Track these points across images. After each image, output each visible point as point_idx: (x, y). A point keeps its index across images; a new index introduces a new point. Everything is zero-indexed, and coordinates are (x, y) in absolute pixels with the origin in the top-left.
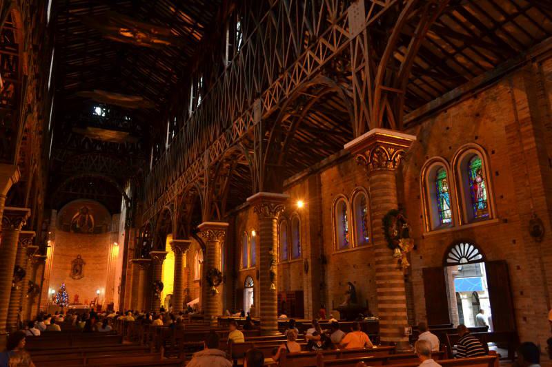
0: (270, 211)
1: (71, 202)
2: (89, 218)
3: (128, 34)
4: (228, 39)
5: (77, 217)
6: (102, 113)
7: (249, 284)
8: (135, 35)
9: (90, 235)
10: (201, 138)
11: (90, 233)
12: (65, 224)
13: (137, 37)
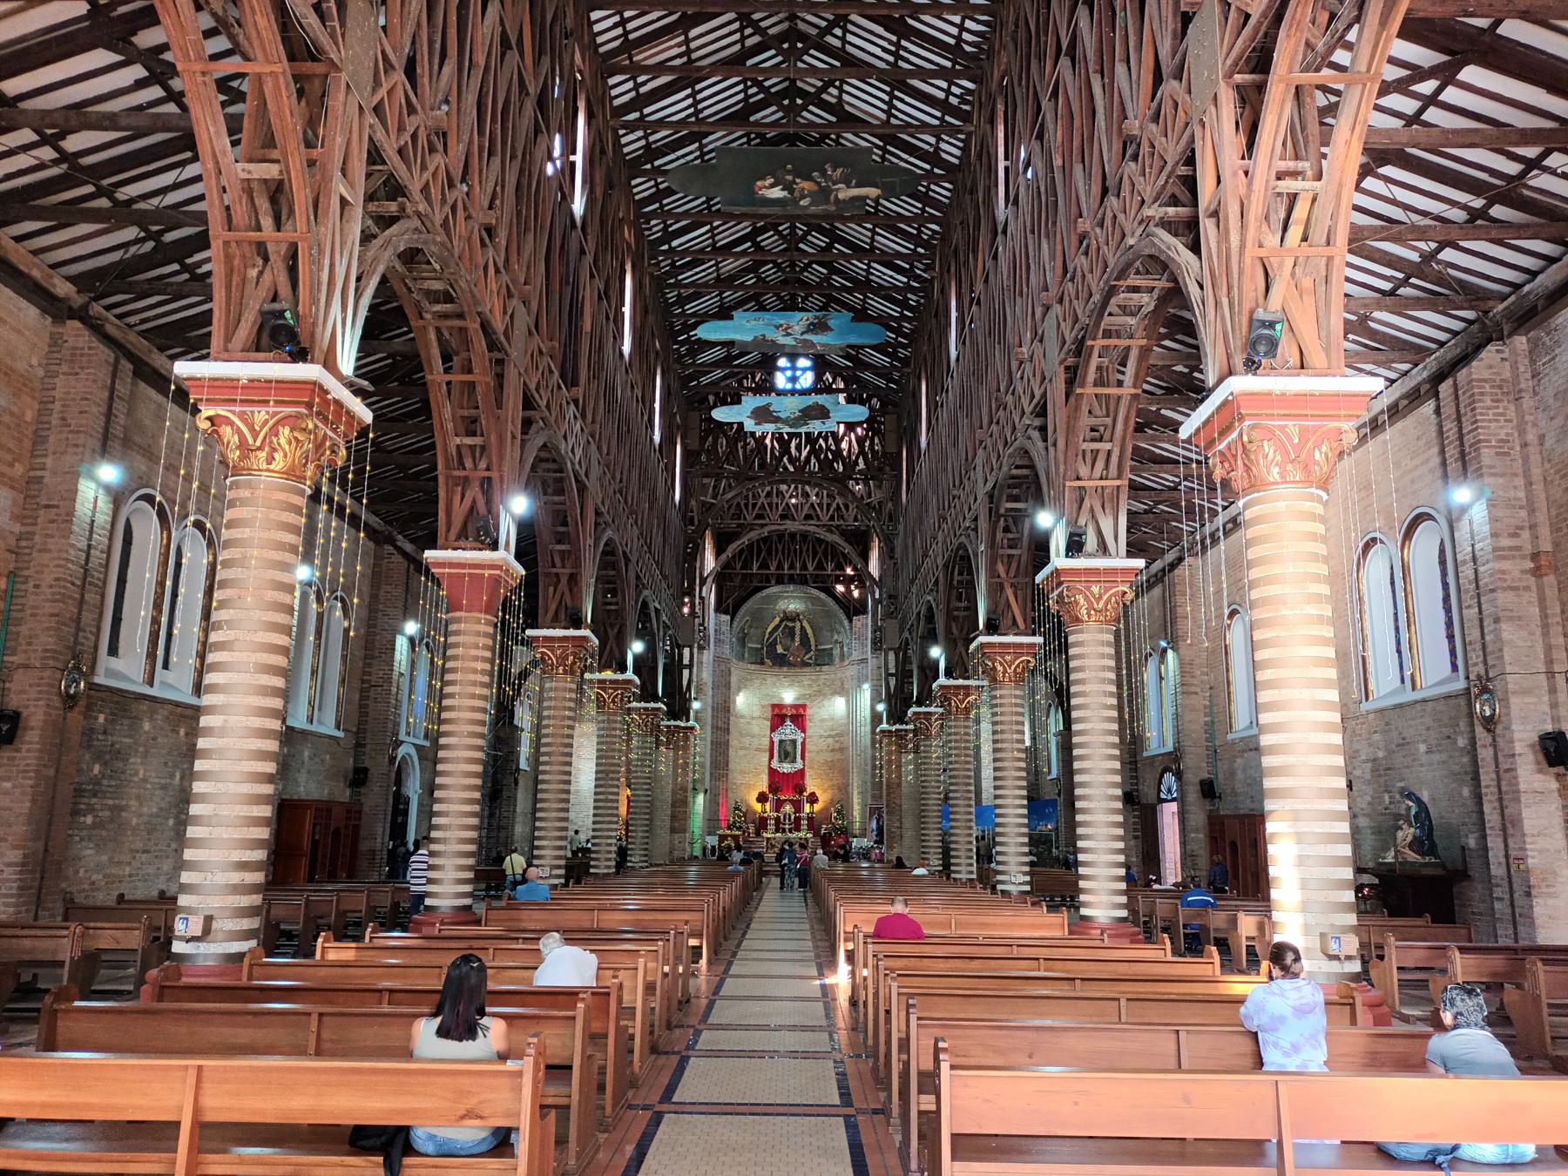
1: (759, 595)
2: (802, 626)
3: (777, 193)
4: (1001, 150)
5: (776, 628)
6: (804, 370)
7: (1169, 791)
8: (791, 191)
9: (807, 669)
10: (969, 415)
11: (808, 665)
13: (797, 194)
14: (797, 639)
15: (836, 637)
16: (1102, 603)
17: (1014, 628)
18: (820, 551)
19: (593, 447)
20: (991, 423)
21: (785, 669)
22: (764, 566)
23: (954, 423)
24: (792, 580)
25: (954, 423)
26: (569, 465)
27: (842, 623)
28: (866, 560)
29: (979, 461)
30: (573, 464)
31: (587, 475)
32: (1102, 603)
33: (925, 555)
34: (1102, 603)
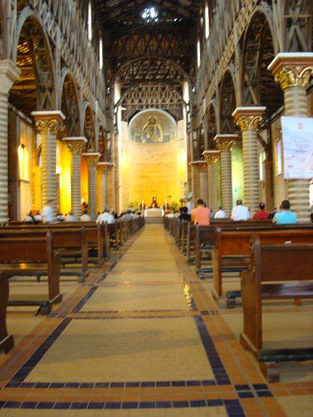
0: (295, 77)
5: (146, 127)
12: (136, 135)
14: (155, 131)
15: (171, 130)
16: (301, 74)
17: (252, 104)
18: (164, 94)
19: (58, 28)
20: (240, 7)
21: (150, 144)
22: (140, 101)
23: (222, 19)
24: (152, 106)
25: (222, 19)
26: (44, 31)
27: (173, 123)
28: (182, 94)
29: (235, 29)
30: (47, 32)
31: (55, 38)
32: (301, 74)
33: (210, 82)
34: (300, 76)
